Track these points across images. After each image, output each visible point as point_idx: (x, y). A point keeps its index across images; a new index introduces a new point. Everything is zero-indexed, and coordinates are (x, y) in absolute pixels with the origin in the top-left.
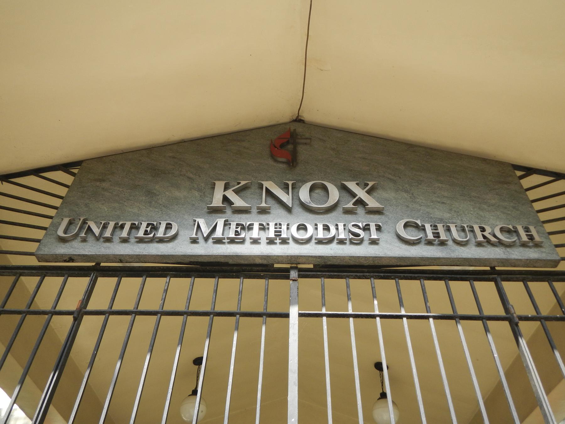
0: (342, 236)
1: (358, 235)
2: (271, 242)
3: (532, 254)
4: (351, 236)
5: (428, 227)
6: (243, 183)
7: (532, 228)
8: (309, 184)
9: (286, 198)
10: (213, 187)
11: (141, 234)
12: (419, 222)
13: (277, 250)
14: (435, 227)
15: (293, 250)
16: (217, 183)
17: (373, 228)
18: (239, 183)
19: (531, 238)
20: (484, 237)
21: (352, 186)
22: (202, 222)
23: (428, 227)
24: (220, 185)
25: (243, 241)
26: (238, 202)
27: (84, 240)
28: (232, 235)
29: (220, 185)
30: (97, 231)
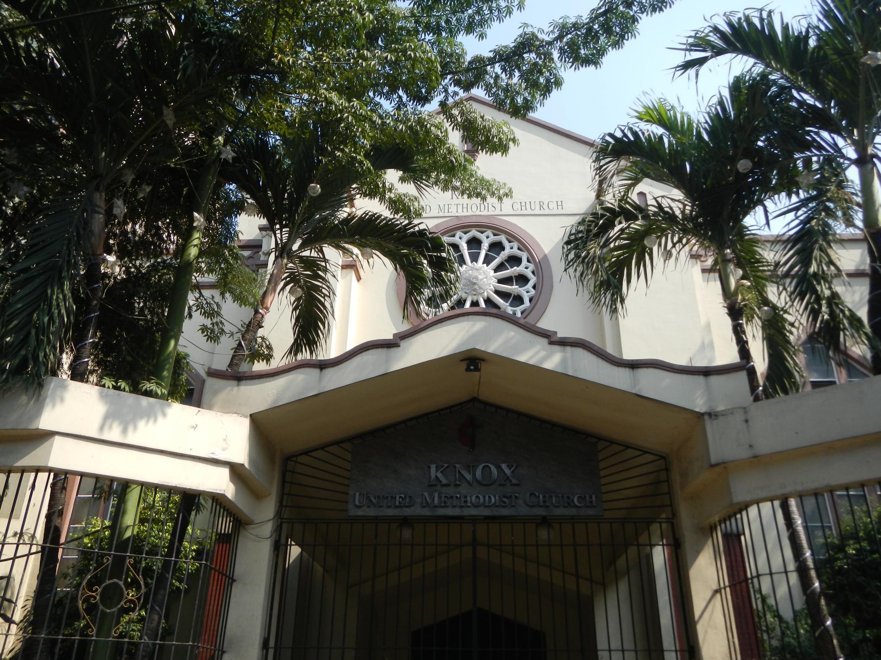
0: (498, 504)
1: (505, 503)
2: (461, 507)
3: (590, 512)
4: (502, 504)
5: (541, 496)
6: (446, 465)
7: (594, 498)
8: (481, 467)
9: (469, 477)
10: (429, 467)
11: (397, 503)
12: (537, 494)
13: (466, 512)
14: (544, 497)
15: (474, 512)
16: (431, 466)
17: (513, 497)
18: (443, 466)
19: (591, 502)
20: (568, 503)
21: (504, 466)
22: (426, 494)
23: (541, 496)
24: (433, 468)
25: (447, 507)
26: (444, 481)
27: (369, 507)
28: (443, 505)
29: (433, 468)
30: (374, 501)
